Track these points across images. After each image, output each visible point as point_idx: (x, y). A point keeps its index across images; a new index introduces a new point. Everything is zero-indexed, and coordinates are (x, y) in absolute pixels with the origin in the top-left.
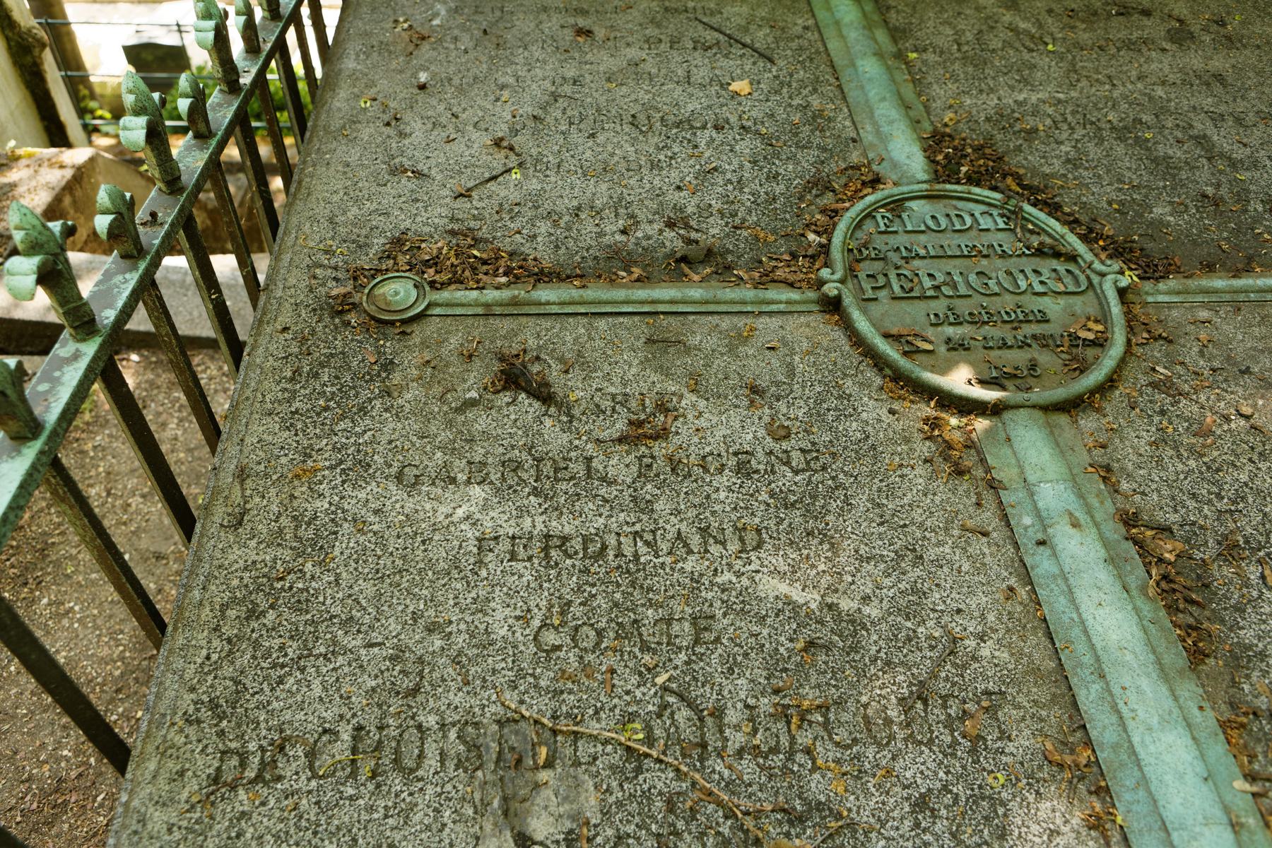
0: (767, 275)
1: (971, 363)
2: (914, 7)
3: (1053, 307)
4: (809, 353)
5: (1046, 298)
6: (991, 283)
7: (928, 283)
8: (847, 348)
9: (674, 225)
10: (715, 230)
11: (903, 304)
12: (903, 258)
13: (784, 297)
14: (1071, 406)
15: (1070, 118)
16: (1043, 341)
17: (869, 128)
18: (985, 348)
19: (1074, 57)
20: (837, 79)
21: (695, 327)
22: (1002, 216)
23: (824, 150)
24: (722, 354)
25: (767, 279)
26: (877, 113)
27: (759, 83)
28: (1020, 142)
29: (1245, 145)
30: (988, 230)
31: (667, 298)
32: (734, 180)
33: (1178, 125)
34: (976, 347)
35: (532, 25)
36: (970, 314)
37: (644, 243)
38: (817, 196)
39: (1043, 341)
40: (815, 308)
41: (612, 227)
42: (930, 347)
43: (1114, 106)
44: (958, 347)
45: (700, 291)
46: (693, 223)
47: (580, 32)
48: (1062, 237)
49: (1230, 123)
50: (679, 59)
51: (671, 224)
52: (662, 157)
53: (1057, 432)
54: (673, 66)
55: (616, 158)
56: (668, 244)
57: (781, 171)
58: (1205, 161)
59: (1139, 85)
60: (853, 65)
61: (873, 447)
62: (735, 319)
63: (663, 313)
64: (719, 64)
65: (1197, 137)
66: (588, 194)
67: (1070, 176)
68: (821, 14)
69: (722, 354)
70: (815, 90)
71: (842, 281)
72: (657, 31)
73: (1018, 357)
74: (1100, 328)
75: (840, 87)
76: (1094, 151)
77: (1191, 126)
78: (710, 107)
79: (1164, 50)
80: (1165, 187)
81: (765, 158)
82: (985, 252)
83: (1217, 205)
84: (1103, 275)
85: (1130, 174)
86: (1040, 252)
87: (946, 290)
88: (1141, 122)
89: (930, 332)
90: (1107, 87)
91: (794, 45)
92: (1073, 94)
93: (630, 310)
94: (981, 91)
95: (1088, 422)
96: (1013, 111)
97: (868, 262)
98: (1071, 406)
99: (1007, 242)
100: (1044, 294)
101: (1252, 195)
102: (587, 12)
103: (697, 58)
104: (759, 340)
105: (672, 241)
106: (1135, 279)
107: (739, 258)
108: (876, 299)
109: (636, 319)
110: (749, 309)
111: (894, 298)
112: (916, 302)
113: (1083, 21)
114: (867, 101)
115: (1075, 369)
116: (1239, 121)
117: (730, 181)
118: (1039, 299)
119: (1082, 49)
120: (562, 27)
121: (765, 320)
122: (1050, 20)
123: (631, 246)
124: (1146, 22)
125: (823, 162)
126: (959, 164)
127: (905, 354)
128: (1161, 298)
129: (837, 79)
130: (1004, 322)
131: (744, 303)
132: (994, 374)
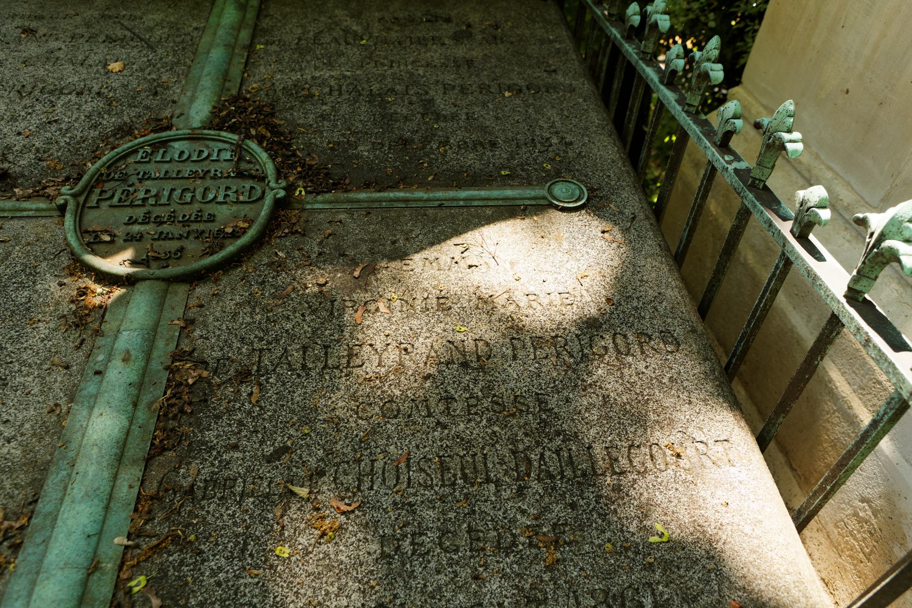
3: (223, 212)
5: (225, 207)
13: (34, 206)
15: (344, 87)
26: (202, 83)
36: (157, 217)
42: (107, 238)
44: (131, 239)
49: (456, 91)
53: (169, 296)
57: (105, 122)
58: (419, 116)
60: (208, 53)
61: (28, 309)
65: (426, 100)
68: (213, 19)
72: (85, 30)
73: (173, 245)
75: (190, 67)
76: (345, 108)
77: (427, 93)
79: (443, 44)
83: (405, 144)
84: (272, 189)
86: (240, 175)
90: (386, 68)
91: (178, 40)
92: (358, 72)
94: (293, 70)
95: (202, 291)
97: (112, 182)
98: (194, 278)
106: (303, 193)
107: (27, 181)
110: (6, 215)
116: (463, 90)
117: (61, 129)
118: (219, 206)
124: (445, 26)
128: (316, 206)
130: (179, 222)
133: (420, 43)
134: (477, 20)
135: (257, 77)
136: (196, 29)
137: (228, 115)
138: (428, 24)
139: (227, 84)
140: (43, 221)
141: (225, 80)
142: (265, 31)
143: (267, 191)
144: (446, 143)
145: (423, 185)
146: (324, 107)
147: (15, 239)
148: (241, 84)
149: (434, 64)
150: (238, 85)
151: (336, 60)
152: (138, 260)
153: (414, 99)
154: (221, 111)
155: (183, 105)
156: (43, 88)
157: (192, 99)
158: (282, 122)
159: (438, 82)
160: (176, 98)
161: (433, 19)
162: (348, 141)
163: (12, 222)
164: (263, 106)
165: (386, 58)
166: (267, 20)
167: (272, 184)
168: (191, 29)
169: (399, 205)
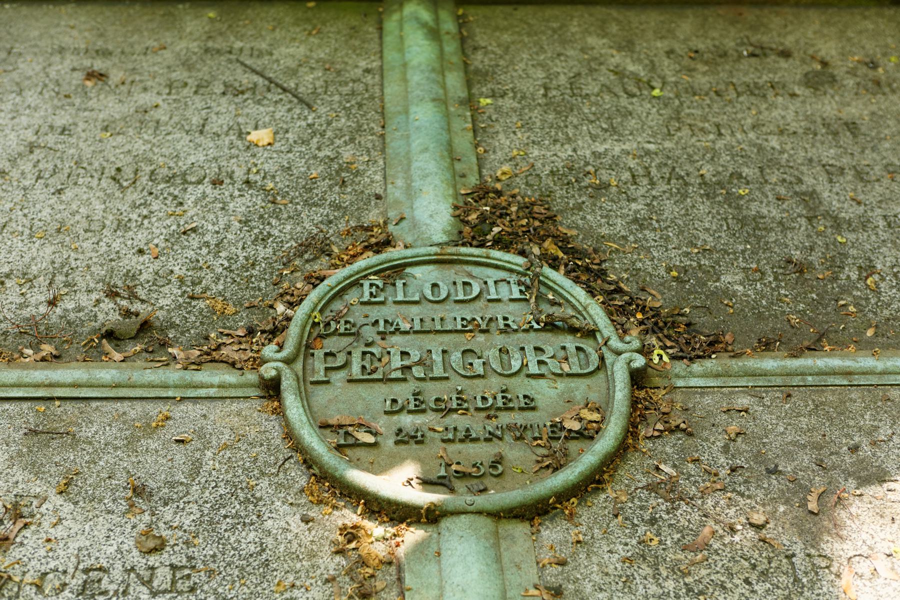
0: (208, 354)
1: (419, 460)
2: (507, 48)
3: (546, 393)
4: (226, 447)
5: (542, 382)
6: (477, 363)
7: (397, 362)
8: (278, 441)
9: (117, 294)
10: (164, 303)
11: (361, 388)
12: (379, 333)
13: (216, 380)
14: (535, 512)
15: (654, 171)
16: (520, 433)
17: (400, 182)
18: (443, 441)
19: (681, 104)
20: (383, 127)
21: (95, 416)
22: (519, 283)
23: (338, 207)
24: (116, 448)
25: (211, 357)
26: (415, 165)
27: (287, 131)
28: (584, 199)
29: (859, 203)
30: (498, 300)
31: (69, 380)
32: (213, 242)
33: (784, 180)
34: (433, 439)
35: (38, 68)
36: (438, 400)
37: (72, 316)
38: (307, 261)
39: (520, 433)
40: (253, 392)
41: (38, 297)
42: (370, 439)
43: (712, 159)
44: (408, 439)
45: (114, 372)
46: (141, 293)
47: (91, 75)
48: (585, 309)
49: (849, 178)
50: (199, 105)
51: (112, 294)
52: (134, 216)
53: (504, 544)
54: (188, 114)
55: (78, 217)
56: (101, 317)
57: (276, 232)
58: (803, 221)
59: (752, 135)
60: (406, 112)
61: (266, 564)
62: (150, 406)
63: (59, 398)
64: (246, 111)
65: (804, 194)
66: (27, 259)
67: (631, 238)
68: (391, 55)
69: (116, 448)
70: (352, 140)
71: (288, 361)
72: (186, 74)
73: (483, 452)
74: (596, 416)
75: (382, 136)
76: (670, 209)
77: (800, 181)
78: (216, 159)
79: (793, 95)
80: (743, 252)
81: (261, 217)
82: (484, 327)
83: (801, 272)
84: (618, 353)
85: (706, 236)
86: (551, 326)
87: (418, 372)
88: (740, 176)
89: (382, 424)
90: (712, 137)
91: (345, 90)
92: (668, 144)
93: (20, 394)
94: (556, 141)
95: (553, 533)
96: (587, 164)
97: (335, 338)
98: (535, 512)
99: (519, 315)
100: (541, 376)
101: (850, 261)
102: (110, 54)
103: (224, 104)
104: (172, 432)
105: (109, 314)
106: (666, 358)
107: (182, 333)
108: (328, 382)
109: (25, 405)
110: (170, 394)
111: (349, 381)
112: (377, 386)
113: (706, 63)
114: (408, 152)
115: (548, 467)
116: (860, 175)
117: (207, 244)
118: (533, 382)
119: (695, 94)
120: (74, 70)
121: (188, 407)
122: (666, 62)
123: (54, 319)
124: (783, 63)
125: (330, 222)
126: (494, 224)
127: (339, 448)
128: (693, 382)
129: (383, 127)
130: (478, 409)
131: (166, 386)
132: (442, 473)
133: (752, 94)
134: (834, 53)
135: (499, 153)
136: (368, 71)
137: (483, 218)
138: (753, 60)
139: (458, 166)
140: (235, 406)
141: (453, 159)
142: (484, 75)
143: (609, 357)
144: (868, 269)
145: (864, 345)
146: (634, 206)
147: (200, 438)
148: (480, 167)
149: (792, 130)
150: (476, 168)
151: (621, 124)
152: (433, 477)
153: (782, 191)
154: (467, 213)
155: (397, 202)
156: (152, 172)
157: (410, 192)
158: (574, 232)
159: (811, 160)
160: (379, 191)
161: (759, 52)
162: (700, 266)
163: (182, 407)
164: (533, 204)
165: (705, 119)
166: (479, 56)
167: (615, 343)
168: (359, 72)
169: (837, 382)
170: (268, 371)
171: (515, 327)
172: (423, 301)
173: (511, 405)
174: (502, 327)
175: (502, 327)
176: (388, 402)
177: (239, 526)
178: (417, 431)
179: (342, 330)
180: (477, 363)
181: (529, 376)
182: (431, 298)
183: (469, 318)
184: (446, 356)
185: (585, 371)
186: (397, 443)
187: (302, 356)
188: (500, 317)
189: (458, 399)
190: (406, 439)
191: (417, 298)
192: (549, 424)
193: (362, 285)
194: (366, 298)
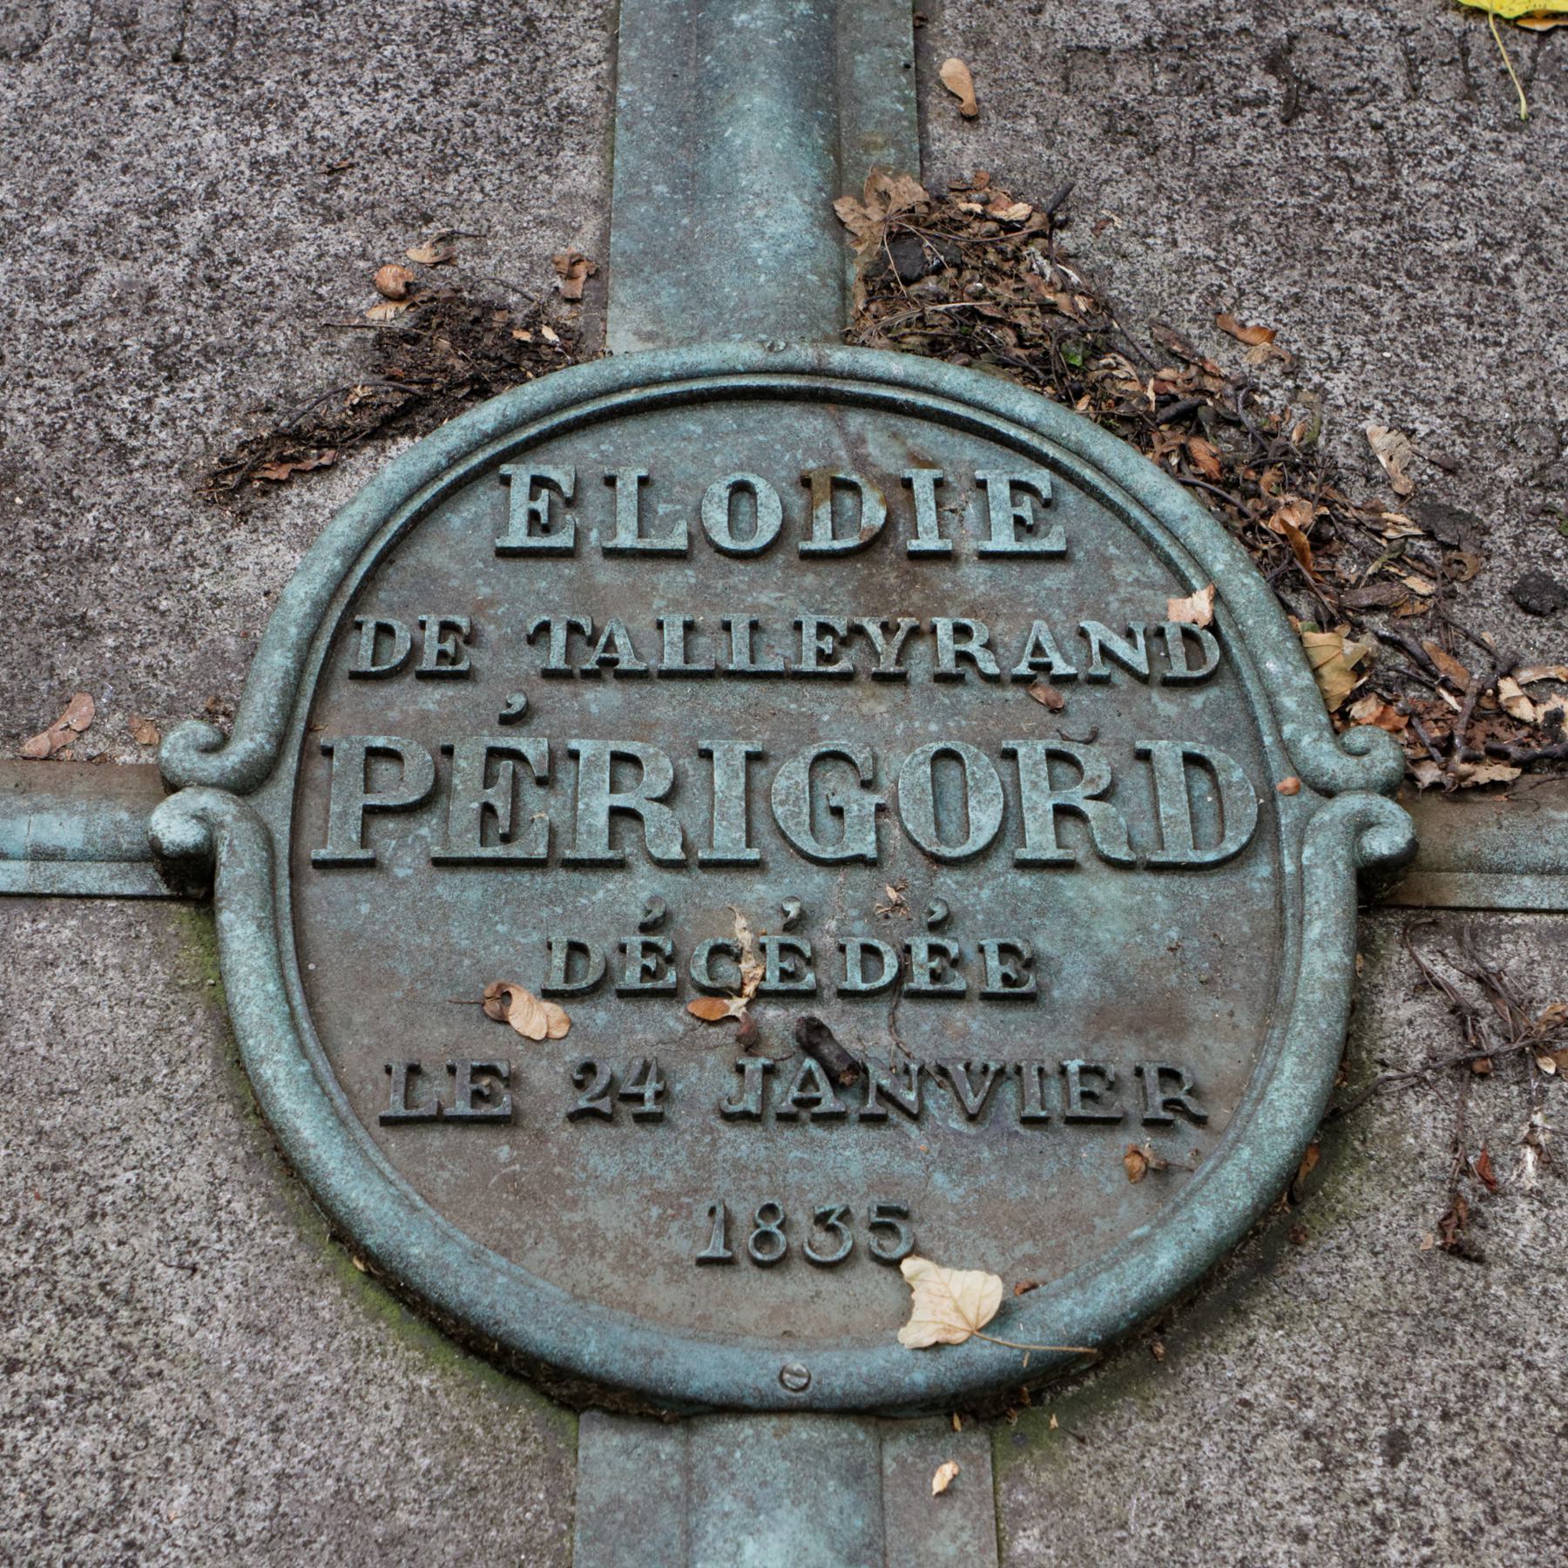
11: (473, 888)
82: (888, 666)
108: (370, 864)
170: (174, 826)
171: (992, 669)
172: (704, 556)
173: (958, 984)
174: (947, 663)
175: (947, 663)
176: (559, 958)
177: (50, 1404)
178: (642, 1079)
179: (428, 662)
180: (861, 804)
181: (1023, 865)
182: (727, 542)
183: (841, 627)
184: (761, 772)
185: (1211, 857)
186: (577, 1117)
187: (291, 762)
188: (944, 626)
189: (785, 949)
190: (604, 1105)
191: (679, 542)
192: (1074, 1066)
193: (506, 481)
194: (518, 536)
